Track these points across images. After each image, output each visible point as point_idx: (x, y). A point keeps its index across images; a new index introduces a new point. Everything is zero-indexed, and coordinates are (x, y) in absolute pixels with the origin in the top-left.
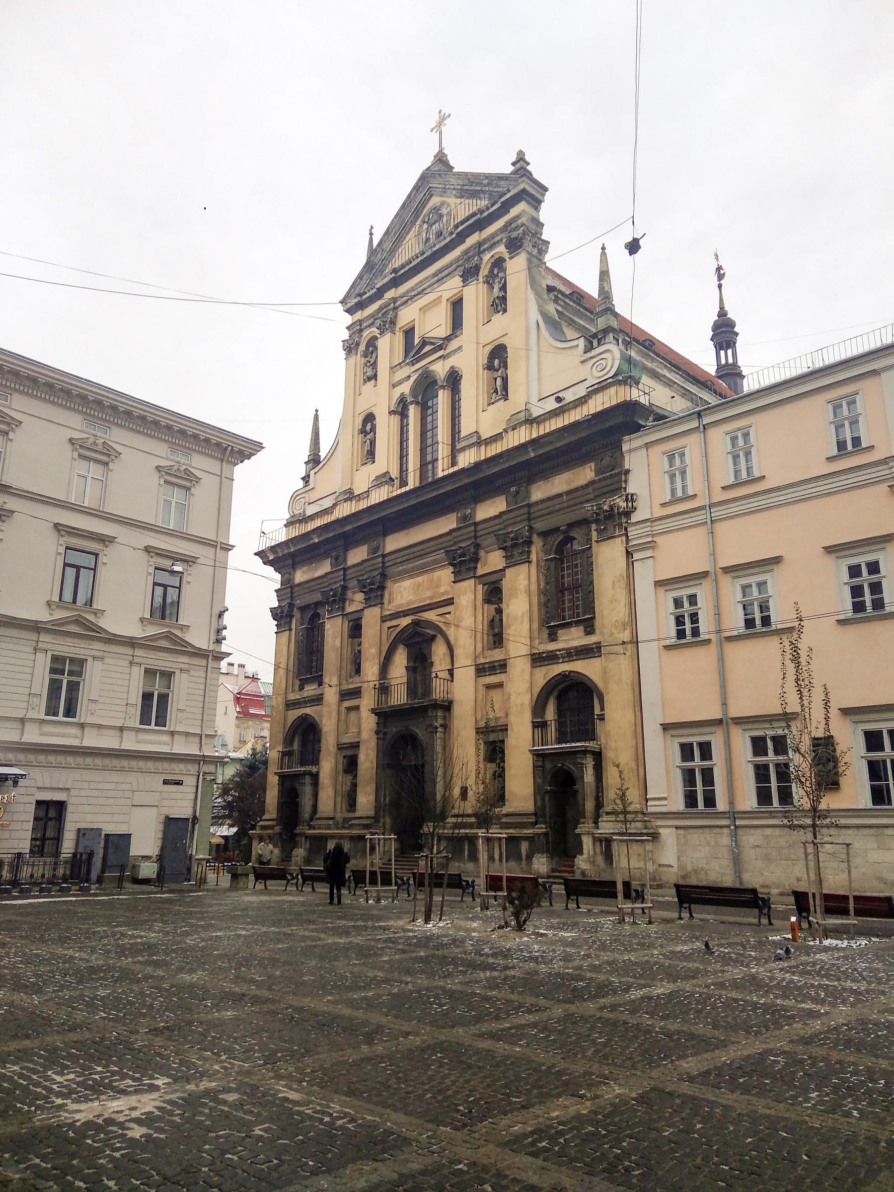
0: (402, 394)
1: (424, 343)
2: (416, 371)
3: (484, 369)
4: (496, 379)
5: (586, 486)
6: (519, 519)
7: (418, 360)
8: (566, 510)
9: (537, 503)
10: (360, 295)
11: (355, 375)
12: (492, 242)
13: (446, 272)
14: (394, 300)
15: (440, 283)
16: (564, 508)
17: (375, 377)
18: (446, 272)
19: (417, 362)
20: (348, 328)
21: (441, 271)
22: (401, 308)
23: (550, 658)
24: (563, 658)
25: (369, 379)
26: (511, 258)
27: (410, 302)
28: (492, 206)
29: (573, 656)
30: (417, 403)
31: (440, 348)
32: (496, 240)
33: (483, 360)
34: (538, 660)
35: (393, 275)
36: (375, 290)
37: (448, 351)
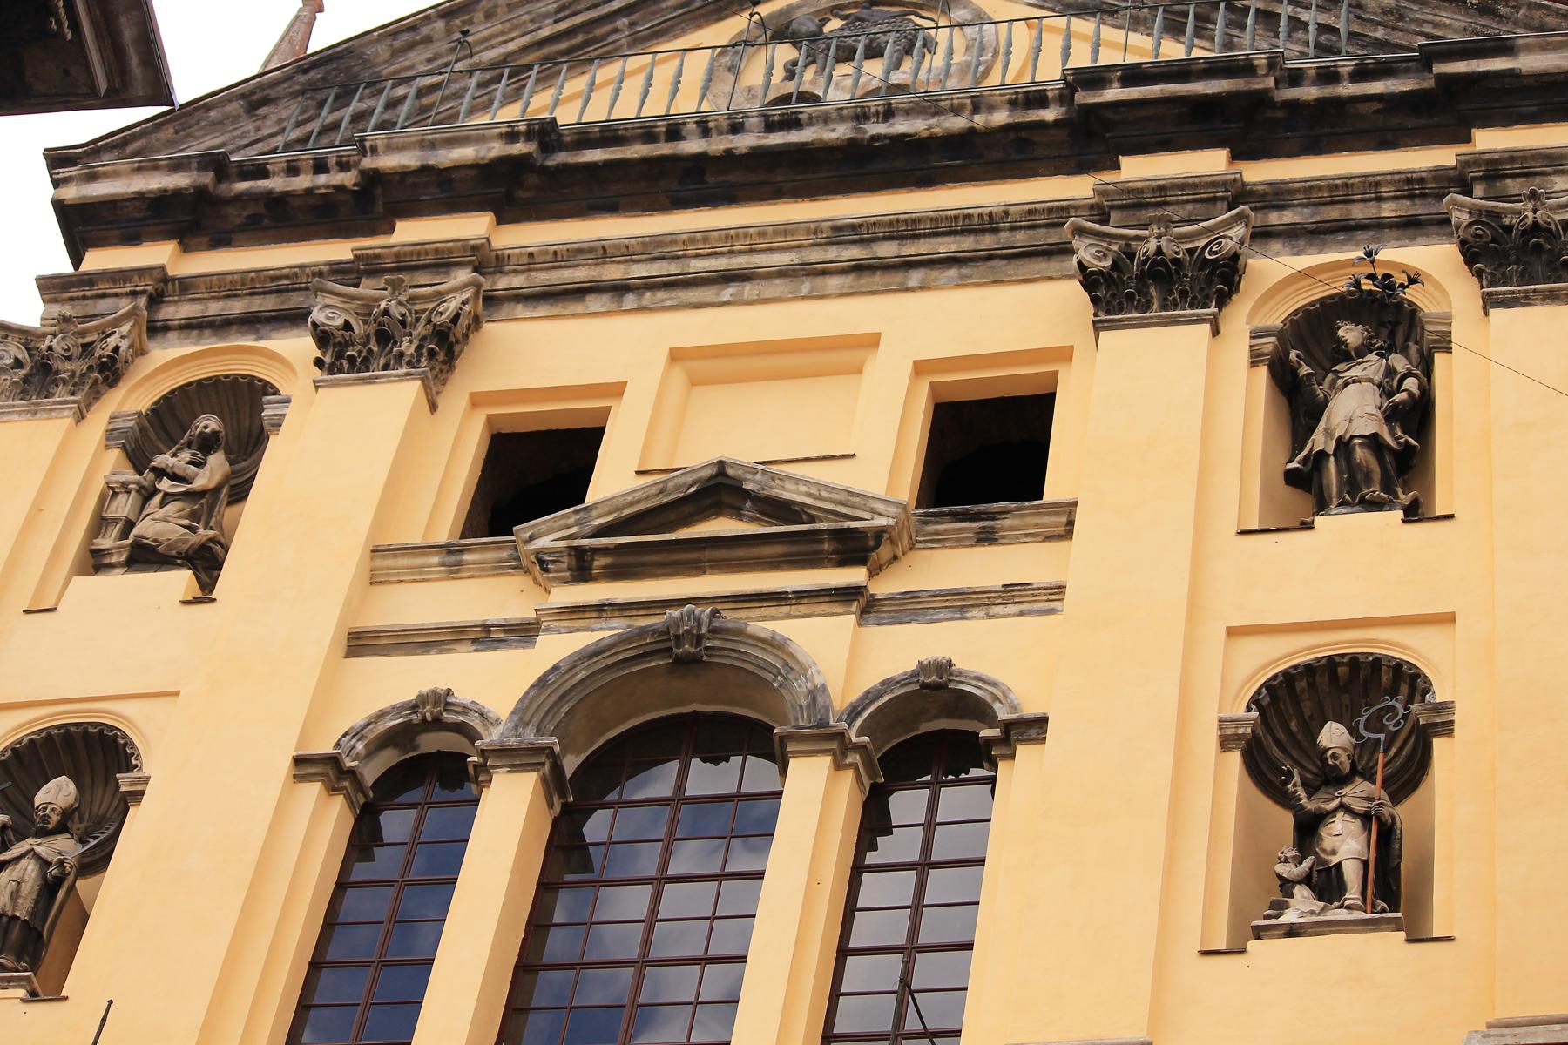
0: (442, 699)
1: (720, 489)
2: (600, 610)
3: (1226, 743)
4: (1321, 818)
7: (626, 565)
10: (217, 164)
11: (37, 509)
12: (1334, 213)
13: (946, 246)
14: (484, 260)
15: (878, 279)
17: (206, 563)
18: (946, 246)
19: (617, 573)
20: (51, 287)
21: (907, 229)
22: (520, 310)
25: (145, 557)
26: (1489, 302)
27: (595, 303)
28: (1361, 74)
30: (555, 783)
31: (854, 546)
32: (1358, 212)
33: (1234, 681)
35: (520, 148)
36: (348, 179)
37: (885, 587)
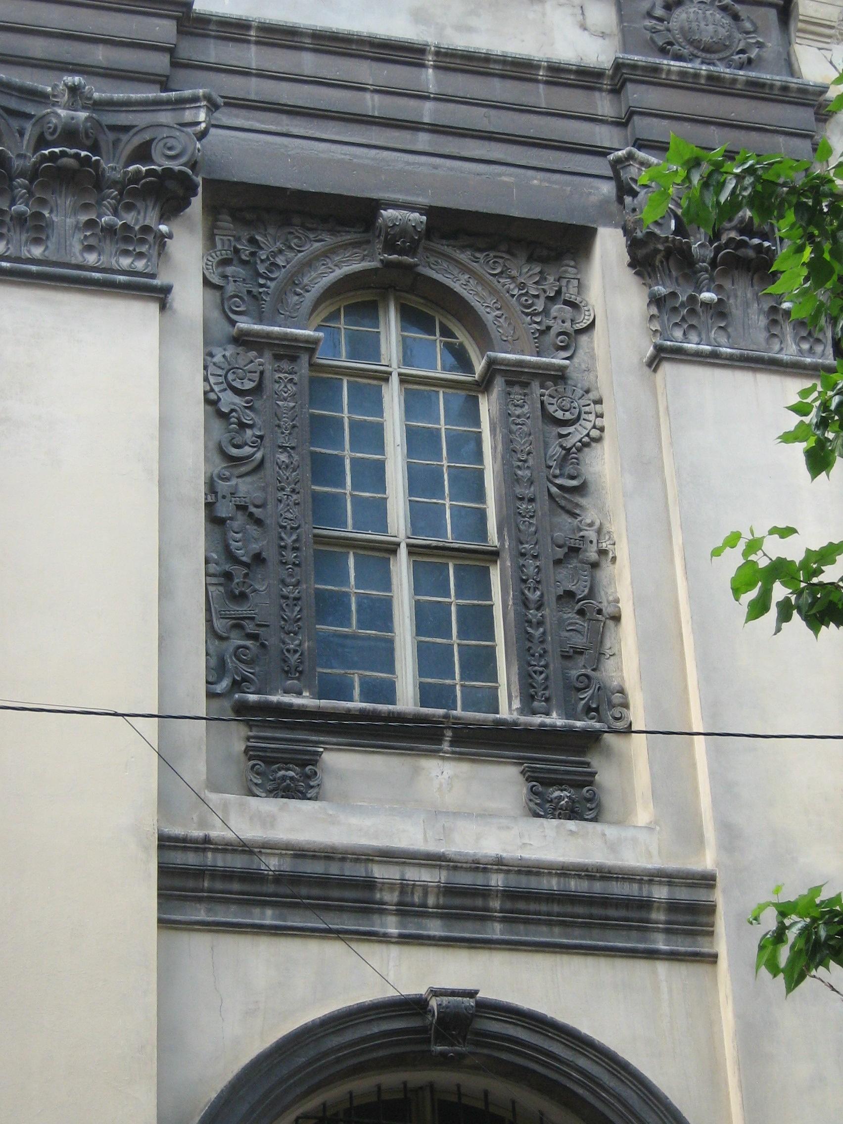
5: (585, 78)
6: (100, 55)
8: (423, 141)
9: (234, 30)
16: (415, 126)
23: (327, 895)
24: (404, 910)
29: (483, 917)
34: (203, 886)
